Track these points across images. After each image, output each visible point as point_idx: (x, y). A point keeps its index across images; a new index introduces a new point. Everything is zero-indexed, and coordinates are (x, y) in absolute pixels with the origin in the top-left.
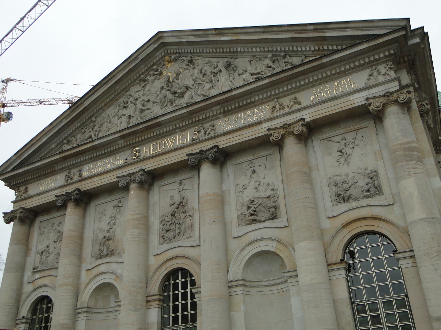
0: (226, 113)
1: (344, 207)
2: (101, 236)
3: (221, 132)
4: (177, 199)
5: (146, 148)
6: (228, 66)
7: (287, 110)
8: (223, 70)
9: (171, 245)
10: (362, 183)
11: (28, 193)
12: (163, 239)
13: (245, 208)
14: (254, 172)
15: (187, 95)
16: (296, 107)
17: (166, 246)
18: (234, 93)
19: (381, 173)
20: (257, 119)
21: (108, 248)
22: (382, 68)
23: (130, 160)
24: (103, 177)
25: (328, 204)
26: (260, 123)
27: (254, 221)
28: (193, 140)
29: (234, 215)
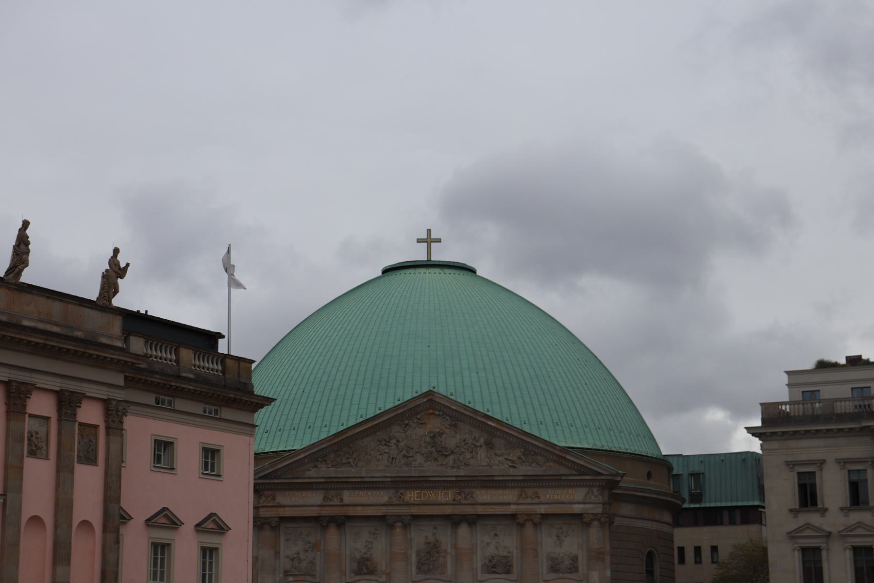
0: (483, 487)
1: (553, 576)
4: (431, 539)
5: (411, 494)
7: (529, 501)
8: (484, 447)
9: (427, 577)
10: (567, 562)
11: (277, 501)
12: (419, 569)
13: (487, 562)
14: (496, 535)
15: (451, 458)
16: (537, 500)
18: (496, 478)
19: (580, 558)
20: (506, 498)
21: (367, 568)
22: (595, 490)
24: (367, 508)
25: (545, 571)
26: (509, 504)
27: (494, 572)
28: (454, 500)
29: (479, 564)
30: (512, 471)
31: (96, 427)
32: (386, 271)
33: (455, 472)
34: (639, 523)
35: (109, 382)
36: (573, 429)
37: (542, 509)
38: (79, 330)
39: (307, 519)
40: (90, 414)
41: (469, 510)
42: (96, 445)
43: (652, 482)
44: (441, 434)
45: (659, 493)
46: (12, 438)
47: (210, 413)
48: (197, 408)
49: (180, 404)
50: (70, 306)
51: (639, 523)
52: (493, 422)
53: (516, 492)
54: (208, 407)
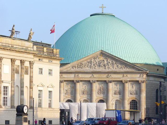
1: (131, 95)
2: (83, 90)
3: (113, 77)
6: (115, 63)
16: (128, 77)
17: (99, 95)
18: (117, 72)
23: (92, 77)
30: (121, 70)
31: (28, 67)
32: (91, 16)
33: (107, 70)
34: (154, 82)
35: (30, 57)
36: (138, 59)
37: (129, 79)
38: (24, 47)
39: (71, 81)
40: (27, 64)
41: (110, 79)
42: (28, 70)
43: (158, 71)
44: (103, 60)
45: (160, 74)
46: (13, 70)
47: (50, 61)
48: (47, 60)
49: (45, 60)
50: (23, 42)
51: (154, 82)
52: (117, 58)
53: (122, 75)
54: (50, 60)
